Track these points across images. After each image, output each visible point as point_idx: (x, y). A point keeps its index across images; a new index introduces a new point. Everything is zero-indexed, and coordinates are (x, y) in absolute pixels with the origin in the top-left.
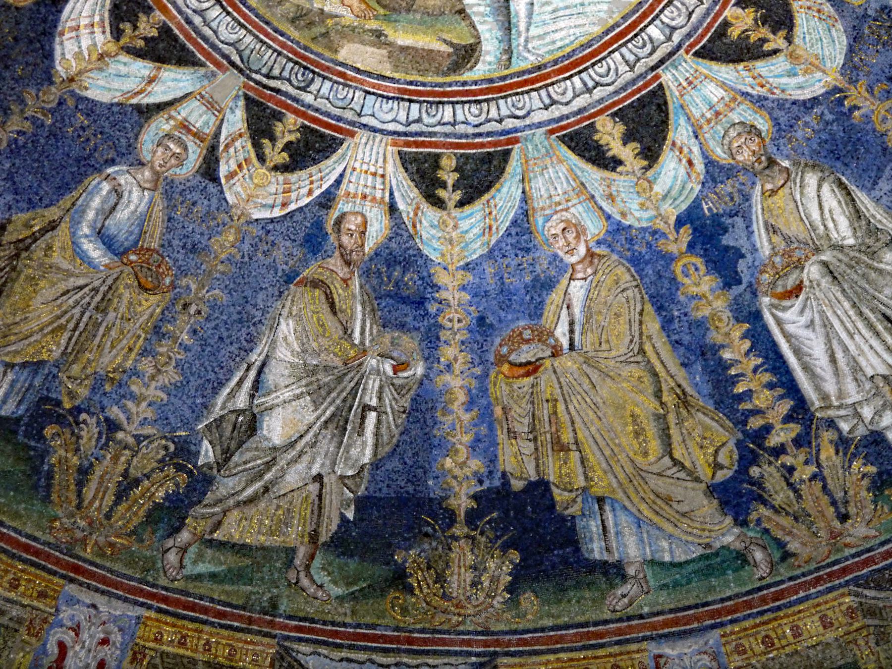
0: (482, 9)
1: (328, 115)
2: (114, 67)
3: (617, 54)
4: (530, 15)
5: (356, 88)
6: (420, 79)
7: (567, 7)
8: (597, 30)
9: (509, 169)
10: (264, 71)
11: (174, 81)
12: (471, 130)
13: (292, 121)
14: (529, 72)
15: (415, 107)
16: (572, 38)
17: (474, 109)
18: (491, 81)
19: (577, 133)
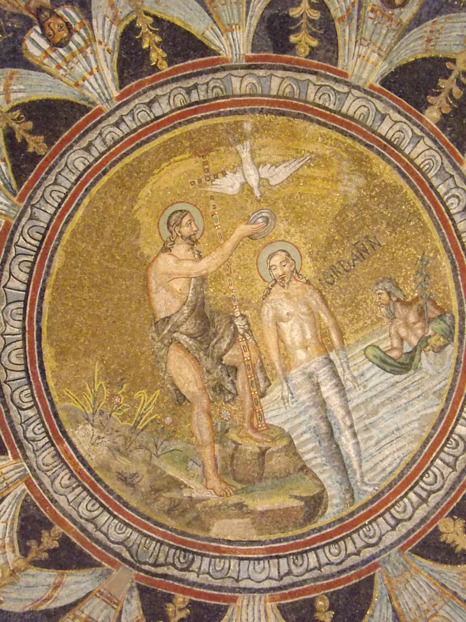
0: (319, 460)
1: (211, 587)
2: (23, 580)
3: (438, 461)
4: (359, 453)
5: (231, 558)
6: (282, 535)
7: (386, 437)
8: (416, 446)
9: (376, 594)
10: (151, 561)
11: (76, 584)
12: (335, 569)
13: (181, 600)
14: (372, 501)
15: (283, 561)
16: (398, 461)
17: (334, 550)
18: (341, 520)
19: (424, 541)
